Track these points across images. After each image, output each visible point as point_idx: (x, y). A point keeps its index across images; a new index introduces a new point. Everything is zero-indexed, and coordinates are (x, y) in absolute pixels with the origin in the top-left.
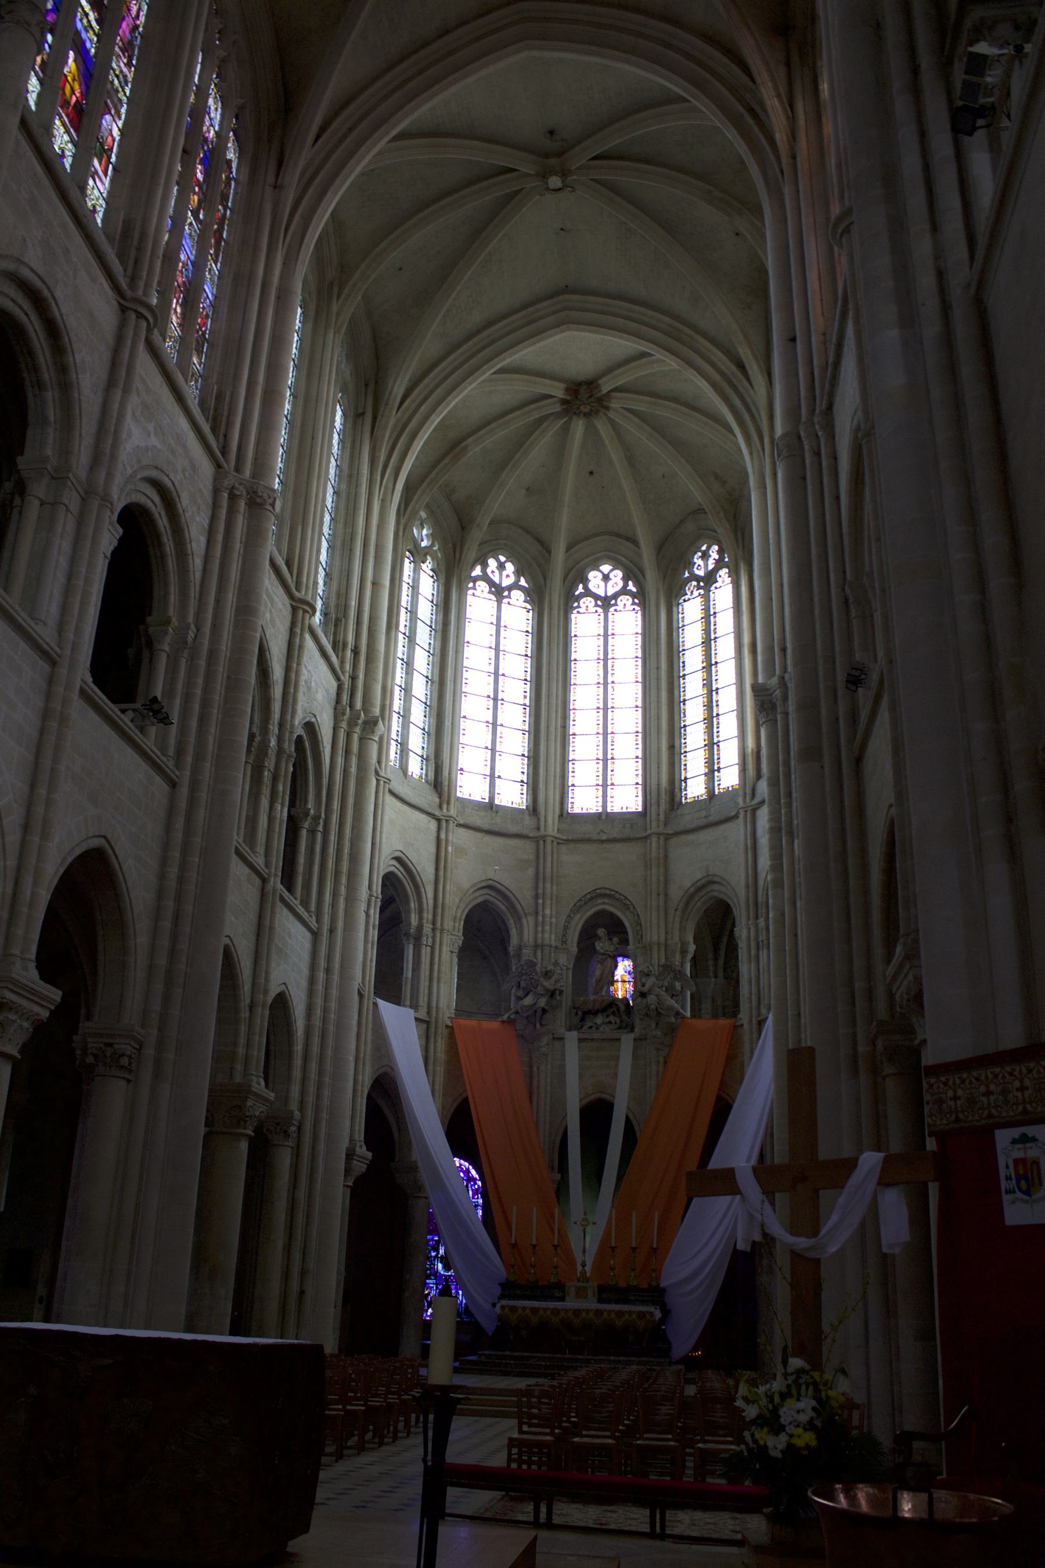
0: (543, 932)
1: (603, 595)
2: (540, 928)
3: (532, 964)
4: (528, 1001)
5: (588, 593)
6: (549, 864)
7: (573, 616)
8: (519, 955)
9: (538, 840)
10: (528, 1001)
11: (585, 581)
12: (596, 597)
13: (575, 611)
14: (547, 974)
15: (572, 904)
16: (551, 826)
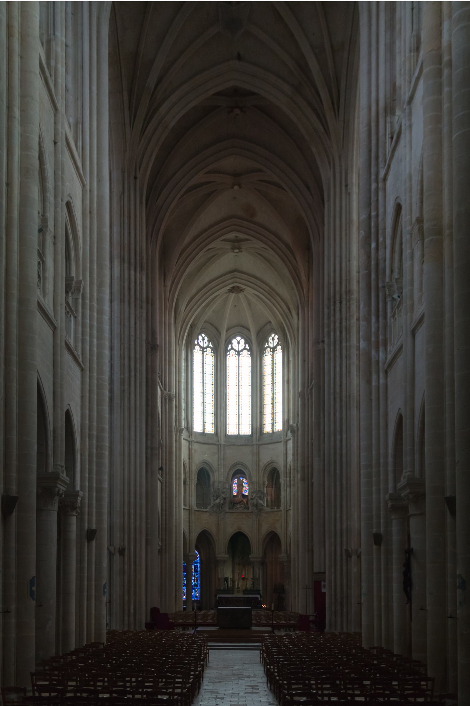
0: (221, 477)
1: (238, 350)
2: (220, 476)
3: (219, 489)
4: (218, 501)
5: (232, 349)
6: (222, 454)
7: (228, 357)
8: (213, 485)
9: (219, 445)
10: (218, 501)
11: (232, 344)
12: (235, 351)
13: (228, 356)
14: (223, 493)
15: (229, 467)
16: (222, 441)
